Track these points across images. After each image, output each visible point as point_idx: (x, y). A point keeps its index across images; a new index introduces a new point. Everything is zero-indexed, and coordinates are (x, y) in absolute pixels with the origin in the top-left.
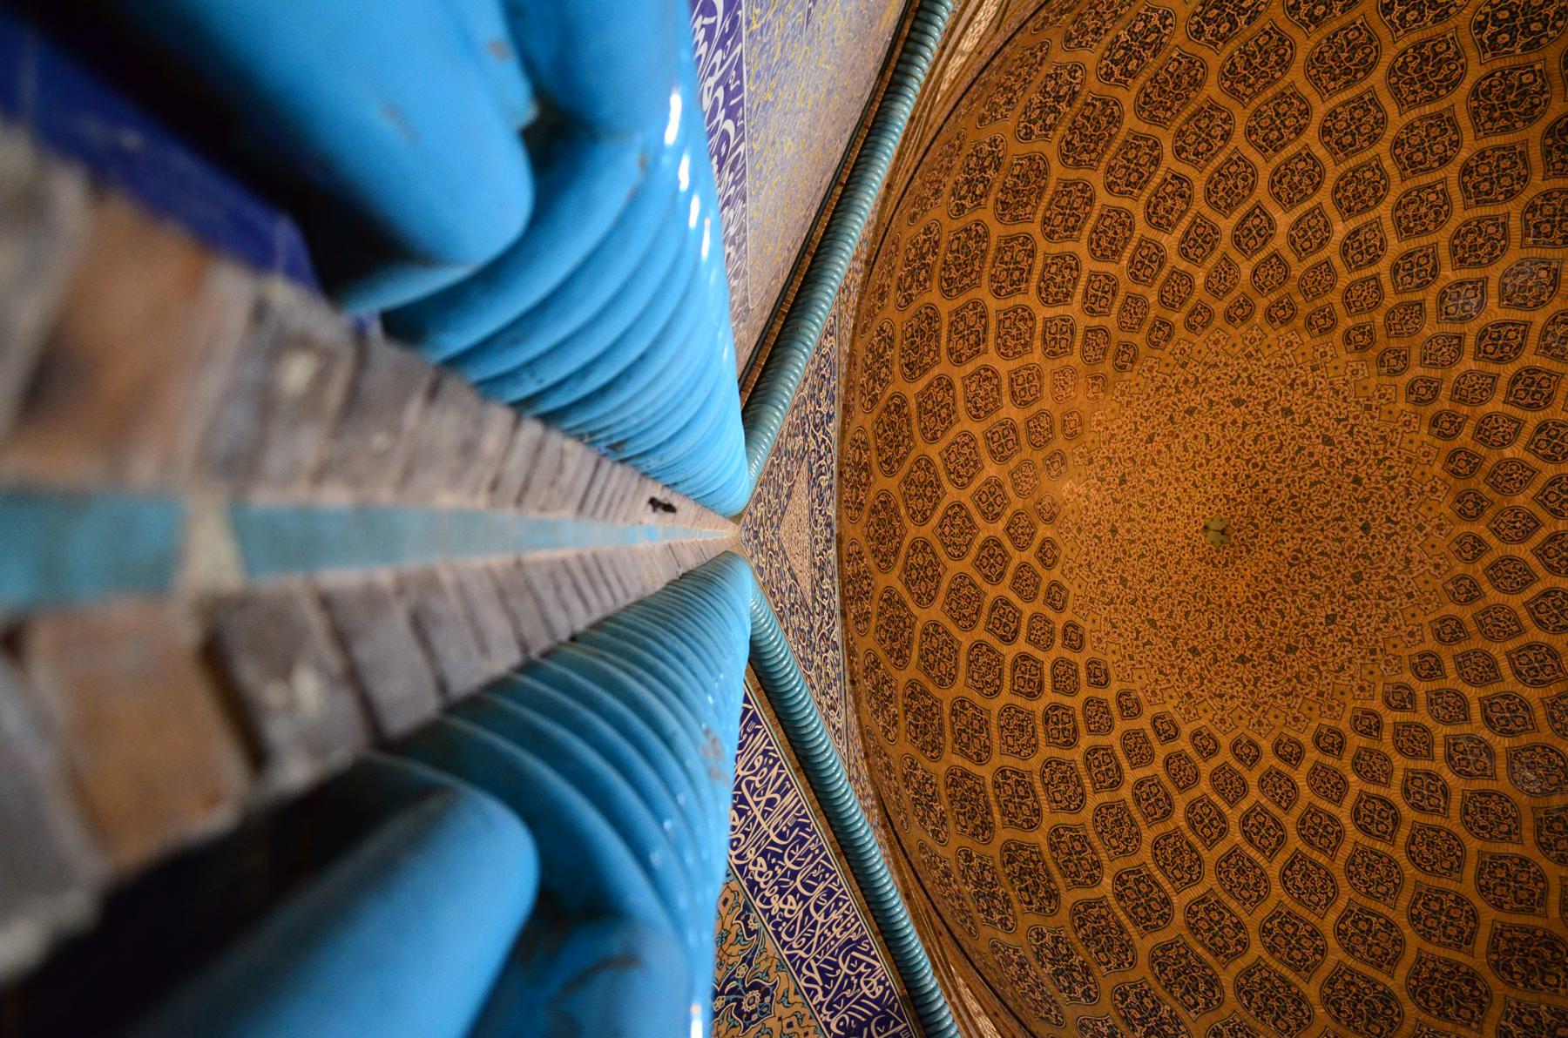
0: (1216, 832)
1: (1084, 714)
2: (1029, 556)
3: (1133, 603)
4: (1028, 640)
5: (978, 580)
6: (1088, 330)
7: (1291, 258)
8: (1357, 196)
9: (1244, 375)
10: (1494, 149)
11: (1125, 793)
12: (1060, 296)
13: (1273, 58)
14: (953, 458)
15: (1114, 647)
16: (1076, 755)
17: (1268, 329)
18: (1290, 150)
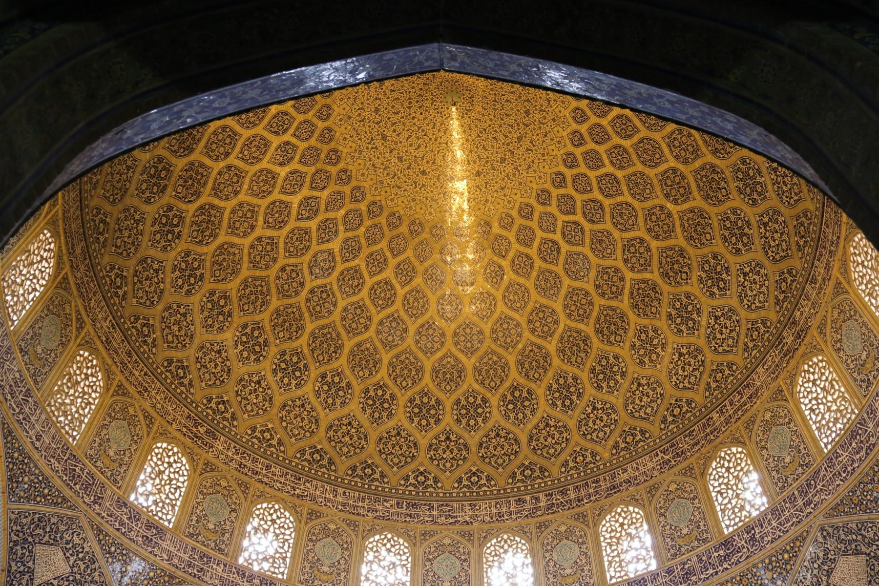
0: (629, 124)
1: (583, 193)
2: (511, 236)
3: (512, 153)
4: (554, 232)
5: (534, 274)
6: (395, 256)
7: (308, 179)
8: (266, 182)
9: (370, 146)
10: (210, 157)
11: (620, 174)
12: (389, 287)
13: (247, 291)
14: (484, 313)
15: (541, 167)
16: (607, 202)
17: (344, 155)
18: (269, 233)
